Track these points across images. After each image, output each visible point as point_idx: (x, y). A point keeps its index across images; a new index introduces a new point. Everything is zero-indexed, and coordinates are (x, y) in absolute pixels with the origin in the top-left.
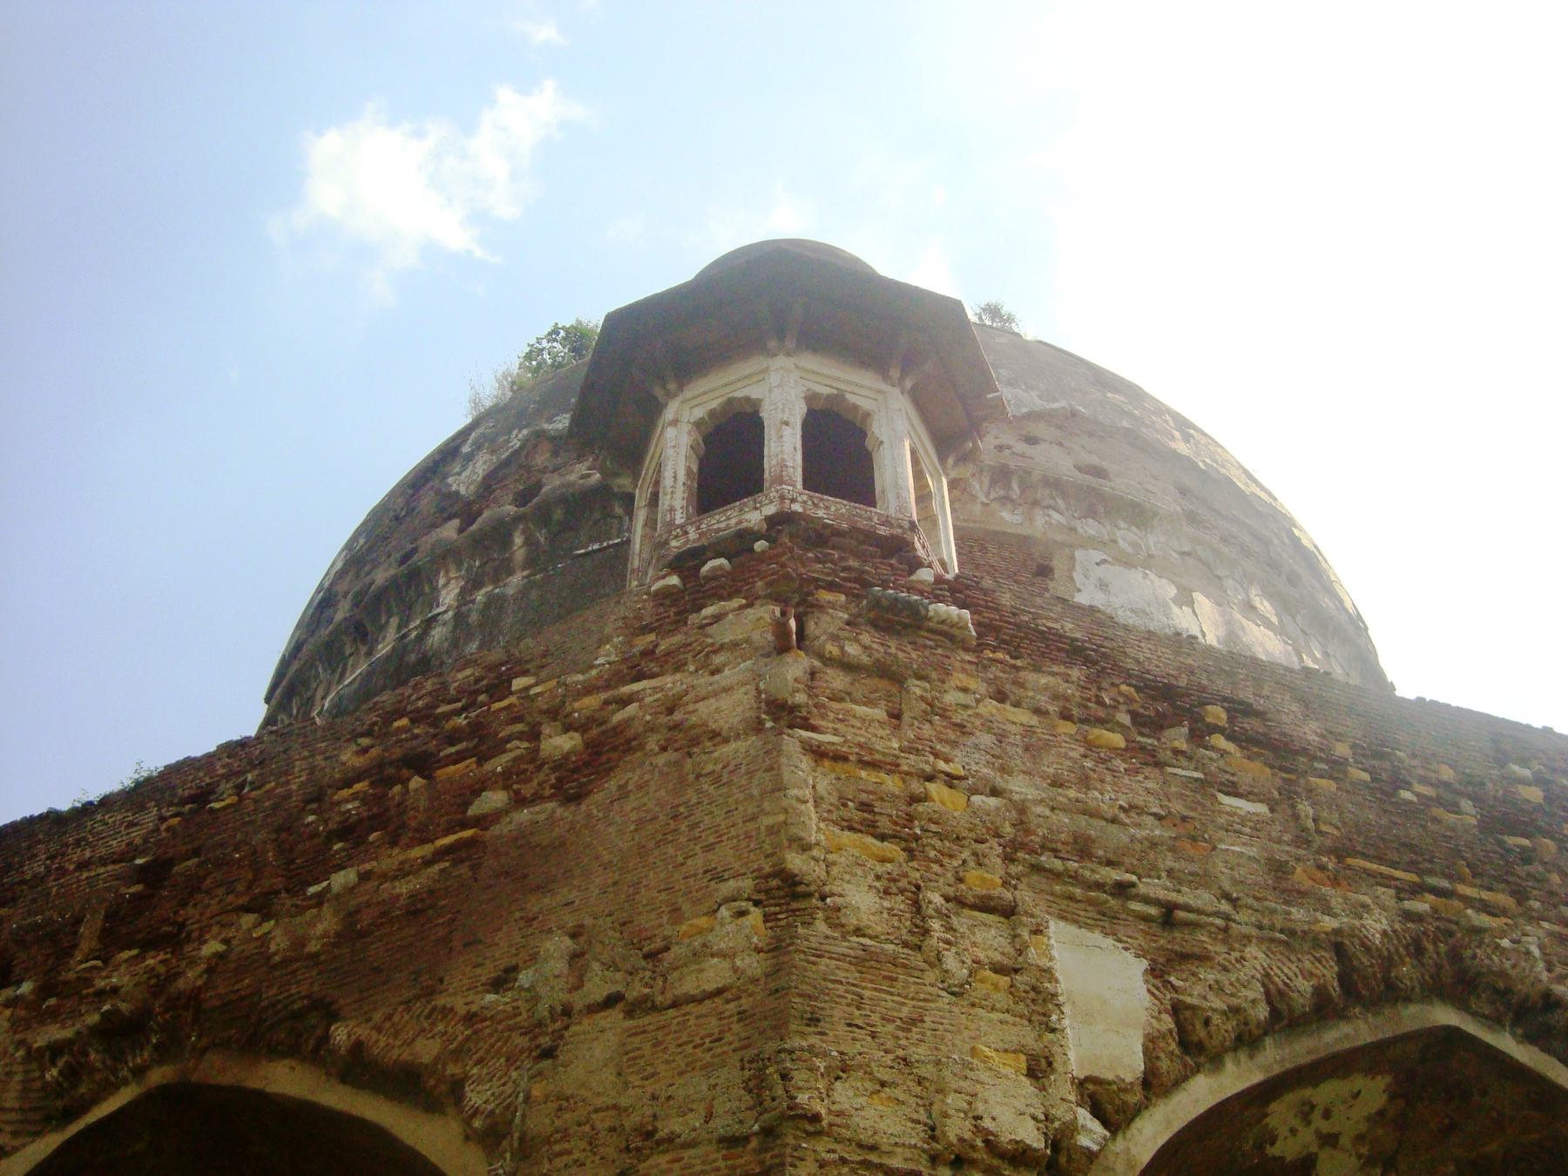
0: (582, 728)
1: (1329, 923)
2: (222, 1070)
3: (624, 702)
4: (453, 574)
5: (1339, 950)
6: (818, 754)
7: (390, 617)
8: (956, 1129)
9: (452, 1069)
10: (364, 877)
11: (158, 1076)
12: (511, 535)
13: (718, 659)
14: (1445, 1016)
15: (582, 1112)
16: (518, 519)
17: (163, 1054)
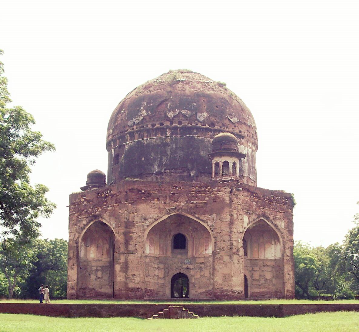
0: (214, 194)
1: (258, 213)
2: (184, 213)
3: (218, 194)
4: (169, 130)
5: (258, 215)
6: (233, 204)
7: (158, 131)
8: (239, 231)
9: (207, 221)
10: (196, 202)
11: (178, 213)
12: (178, 129)
13: (226, 193)
14: (262, 218)
15: (218, 227)
16: (179, 127)
17: (178, 211)
